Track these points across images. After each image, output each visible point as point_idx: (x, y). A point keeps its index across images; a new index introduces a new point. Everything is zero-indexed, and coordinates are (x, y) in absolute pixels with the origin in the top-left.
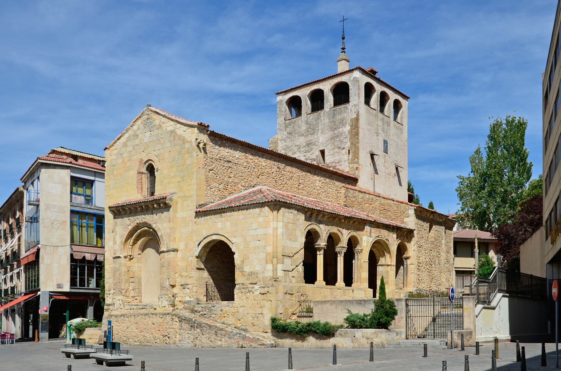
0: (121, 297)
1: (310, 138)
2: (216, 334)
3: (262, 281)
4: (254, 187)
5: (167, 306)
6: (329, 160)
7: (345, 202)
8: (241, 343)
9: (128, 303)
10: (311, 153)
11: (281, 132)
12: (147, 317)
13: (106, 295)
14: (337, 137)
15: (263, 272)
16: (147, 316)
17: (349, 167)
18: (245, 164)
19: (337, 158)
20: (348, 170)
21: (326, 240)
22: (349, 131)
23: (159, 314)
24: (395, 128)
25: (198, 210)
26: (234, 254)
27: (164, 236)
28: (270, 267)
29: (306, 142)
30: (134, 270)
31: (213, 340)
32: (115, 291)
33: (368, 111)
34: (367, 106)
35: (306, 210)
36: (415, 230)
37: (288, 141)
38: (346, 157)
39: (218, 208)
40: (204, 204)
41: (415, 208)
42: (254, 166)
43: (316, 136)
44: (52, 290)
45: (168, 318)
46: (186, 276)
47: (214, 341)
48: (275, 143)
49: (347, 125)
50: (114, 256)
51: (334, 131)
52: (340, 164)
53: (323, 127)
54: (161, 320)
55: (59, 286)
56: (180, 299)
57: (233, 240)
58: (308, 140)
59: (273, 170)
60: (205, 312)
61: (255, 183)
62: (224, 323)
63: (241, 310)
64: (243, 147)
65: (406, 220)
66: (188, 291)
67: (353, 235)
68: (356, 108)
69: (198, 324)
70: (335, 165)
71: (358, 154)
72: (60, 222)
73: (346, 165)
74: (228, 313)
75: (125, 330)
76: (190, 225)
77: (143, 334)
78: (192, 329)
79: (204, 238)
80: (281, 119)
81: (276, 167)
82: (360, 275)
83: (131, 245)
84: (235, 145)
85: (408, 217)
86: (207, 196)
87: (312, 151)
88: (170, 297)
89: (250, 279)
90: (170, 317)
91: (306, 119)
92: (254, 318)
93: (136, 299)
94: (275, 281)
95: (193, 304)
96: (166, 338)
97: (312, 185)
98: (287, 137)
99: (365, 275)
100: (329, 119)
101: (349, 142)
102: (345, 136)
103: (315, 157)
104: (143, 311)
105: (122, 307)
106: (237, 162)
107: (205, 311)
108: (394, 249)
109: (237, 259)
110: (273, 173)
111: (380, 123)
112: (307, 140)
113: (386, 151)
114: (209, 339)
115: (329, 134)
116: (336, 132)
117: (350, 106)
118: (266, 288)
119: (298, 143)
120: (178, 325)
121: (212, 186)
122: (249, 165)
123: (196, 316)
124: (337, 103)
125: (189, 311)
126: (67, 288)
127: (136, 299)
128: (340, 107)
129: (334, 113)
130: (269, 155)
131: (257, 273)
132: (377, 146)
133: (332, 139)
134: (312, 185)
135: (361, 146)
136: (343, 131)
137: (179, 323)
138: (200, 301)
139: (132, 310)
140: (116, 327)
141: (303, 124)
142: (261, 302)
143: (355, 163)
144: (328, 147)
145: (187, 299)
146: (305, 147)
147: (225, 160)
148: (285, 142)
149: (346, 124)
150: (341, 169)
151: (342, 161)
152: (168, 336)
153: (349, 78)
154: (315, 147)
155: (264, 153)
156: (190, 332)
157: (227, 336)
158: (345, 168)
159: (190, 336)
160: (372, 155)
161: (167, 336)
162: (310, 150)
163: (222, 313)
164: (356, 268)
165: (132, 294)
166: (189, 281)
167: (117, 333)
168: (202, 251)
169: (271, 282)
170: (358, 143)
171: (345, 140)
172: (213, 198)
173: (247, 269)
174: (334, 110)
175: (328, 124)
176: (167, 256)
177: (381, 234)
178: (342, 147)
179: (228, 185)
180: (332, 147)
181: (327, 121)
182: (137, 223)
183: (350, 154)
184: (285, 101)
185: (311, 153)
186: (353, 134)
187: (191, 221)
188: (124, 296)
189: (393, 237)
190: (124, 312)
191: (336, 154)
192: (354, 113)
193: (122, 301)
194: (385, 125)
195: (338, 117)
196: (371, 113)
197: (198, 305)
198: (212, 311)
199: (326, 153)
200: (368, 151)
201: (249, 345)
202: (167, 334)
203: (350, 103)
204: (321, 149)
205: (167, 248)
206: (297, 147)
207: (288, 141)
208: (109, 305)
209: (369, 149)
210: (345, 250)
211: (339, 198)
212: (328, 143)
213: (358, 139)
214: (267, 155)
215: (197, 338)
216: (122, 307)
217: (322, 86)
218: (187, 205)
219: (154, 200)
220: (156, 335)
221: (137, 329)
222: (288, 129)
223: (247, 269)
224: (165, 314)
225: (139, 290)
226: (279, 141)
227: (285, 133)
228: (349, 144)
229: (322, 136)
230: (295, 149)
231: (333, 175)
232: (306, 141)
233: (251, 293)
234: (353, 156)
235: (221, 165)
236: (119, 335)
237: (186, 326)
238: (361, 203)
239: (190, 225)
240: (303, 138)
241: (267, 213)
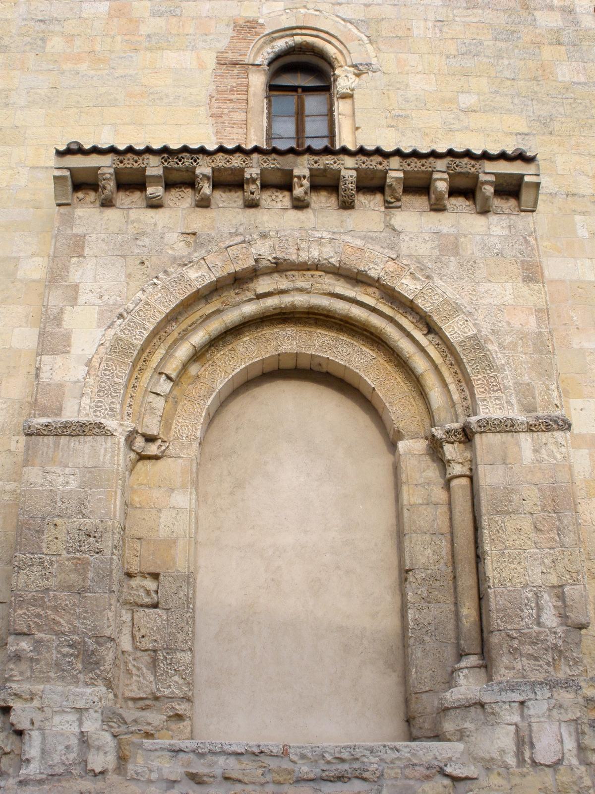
5: (575, 761)
27: (492, 347)
30: (163, 533)
176: (528, 455)
216: (97, 762)
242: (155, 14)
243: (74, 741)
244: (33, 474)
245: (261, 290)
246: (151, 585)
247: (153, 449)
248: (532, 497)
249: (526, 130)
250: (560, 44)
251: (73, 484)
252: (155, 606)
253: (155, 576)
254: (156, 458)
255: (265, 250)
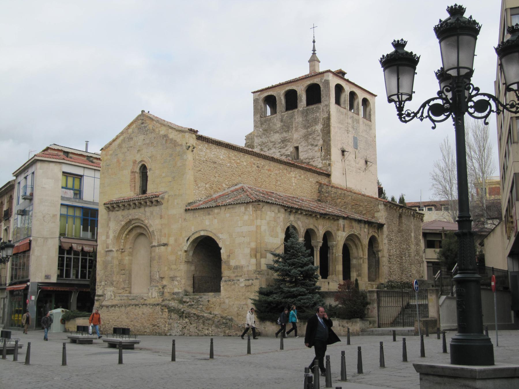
0: (112, 289)
1: (285, 135)
2: (204, 323)
3: (246, 274)
4: (236, 185)
6: (303, 156)
7: (319, 197)
8: (227, 332)
9: (119, 294)
10: (286, 149)
11: (257, 129)
12: (137, 307)
13: (96, 287)
14: (310, 134)
15: (248, 266)
16: (138, 306)
17: (322, 163)
18: (229, 164)
19: (311, 154)
20: (321, 166)
21: (304, 236)
22: (321, 130)
23: (149, 304)
24: (364, 125)
25: (187, 208)
26: (221, 249)
27: (155, 232)
28: (253, 261)
29: (280, 139)
31: (200, 329)
32: (106, 282)
33: (338, 110)
34: (339, 107)
35: (286, 208)
36: (385, 224)
37: (264, 137)
38: (318, 154)
39: (207, 207)
40: (193, 202)
41: (385, 203)
42: (236, 166)
43: (290, 133)
44: (40, 281)
45: (158, 308)
46: (175, 269)
47: (202, 330)
48: (251, 139)
49: (320, 124)
50: (107, 250)
51: (307, 129)
52: (313, 160)
53: (297, 125)
54: (151, 310)
55: (47, 277)
56: (169, 290)
57: (221, 236)
58: (283, 136)
59: (254, 169)
60: (193, 303)
61: (237, 182)
62: (210, 313)
63: (227, 301)
64: (227, 149)
65: (376, 215)
66: (176, 283)
67: (328, 230)
68: (327, 108)
69: (186, 314)
70: (308, 161)
71: (330, 151)
72: (51, 215)
73: (319, 161)
74: (215, 304)
75: (116, 320)
76: (180, 222)
77: (133, 324)
78: (181, 318)
79: (193, 234)
80: (257, 117)
81: (256, 166)
82: (335, 268)
83: (123, 240)
84: (220, 147)
85: (378, 212)
86: (195, 195)
87: (287, 148)
88: (160, 289)
89: (235, 272)
90: (160, 308)
91: (280, 117)
92: (239, 308)
93: (127, 290)
94: (258, 274)
95: (181, 295)
96: (156, 327)
97: (288, 182)
98: (263, 133)
99: (340, 267)
100: (302, 118)
101: (321, 139)
102: (318, 134)
103: (289, 153)
104: (133, 302)
105: (113, 297)
106: (221, 163)
107: (193, 302)
108: (366, 241)
109: (223, 253)
110: (253, 171)
111: (350, 121)
112: (282, 137)
113: (356, 146)
114: (196, 328)
115: (303, 132)
116: (309, 130)
117: (321, 106)
118: (251, 281)
119: (273, 140)
120: (167, 315)
121: (199, 185)
122: (232, 165)
123: (184, 306)
124: (309, 102)
125: (177, 302)
126: (54, 279)
127: (127, 290)
128: (313, 106)
129: (307, 112)
130: (250, 155)
131: (242, 267)
132: (348, 143)
133: (305, 136)
134: (288, 182)
135: (332, 143)
136: (316, 130)
137: (169, 313)
138: (188, 292)
139: (123, 301)
140: (107, 317)
141: (278, 122)
142: (245, 294)
143: (327, 159)
144: (301, 144)
145: (176, 290)
146: (279, 143)
147: (211, 161)
148: (261, 138)
149: (318, 123)
150: (314, 165)
151: (316, 157)
152: (158, 325)
153: (321, 80)
154: (289, 143)
155: (245, 154)
156: (179, 322)
157: (214, 325)
158: (318, 163)
159: (178, 325)
160: (343, 152)
161: (156, 325)
162: (285, 146)
163: (209, 304)
164: (331, 262)
165: (123, 285)
166: (178, 274)
167: (108, 322)
168: (191, 246)
169: (255, 275)
170: (330, 140)
171: (318, 138)
172: (200, 196)
173: (233, 263)
174: (306, 110)
175: (302, 122)
177: (353, 229)
178: (315, 144)
179: (213, 184)
180: (306, 144)
181: (301, 119)
182: (130, 219)
183: (323, 151)
184: (261, 99)
185: (286, 149)
186: (325, 132)
187: (181, 218)
188: (115, 287)
189: (365, 232)
190: (115, 302)
191: (310, 151)
192: (325, 113)
193: (113, 292)
194: (355, 123)
195: (311, 117)
196: (341, 112)
197: (186, 297)
198: (199, 302)
199: (300, 149)
200: (339, 148)
201: (234, 333)
202: (156, 323)
203: (322, 104)
204: (296, 145)
205: (158, 242)
206: (272, 143)
207: (264, 137)
208: (100, 296)
209: (340, 146)
210: (320, 244)
211: (313, 193)
212: (301, 140)
213: (330, 137)
214: (248, 155)
215: (185, 327)
217: (295, 87)
218: (177, 204)
219: (147, 198)
220: (145, 324)
221: (127, 318)
222: (264, 126)
223: (233, 263)
224: (155, 305)
225: (129, 282)
226: (255, 137)
227: (261, 130)
228: (321, 142)
229: (296, 133)
230: (271, 145)
231: (307, 172)
232: (280, 138)
233: (237, 285)
234: (325, 153)
235: (207, 166)
236: (110, 324)
237: (174, 316)
238: (334, 199)
239: (180, 220)
240: (278, 135)
241: (251, 212)
242: (123, 161)
243: (110, 295)
244: (107, 258)
245: (133, 223)
246: (124, 271)
247: (123, 251)
248: (157, 257)
249: (171, 180)
250: (179, 156)
251: (110, 259)
252: (124, 274)
253: (124, 270)
254: (124, 252)
255: (130, 217)
